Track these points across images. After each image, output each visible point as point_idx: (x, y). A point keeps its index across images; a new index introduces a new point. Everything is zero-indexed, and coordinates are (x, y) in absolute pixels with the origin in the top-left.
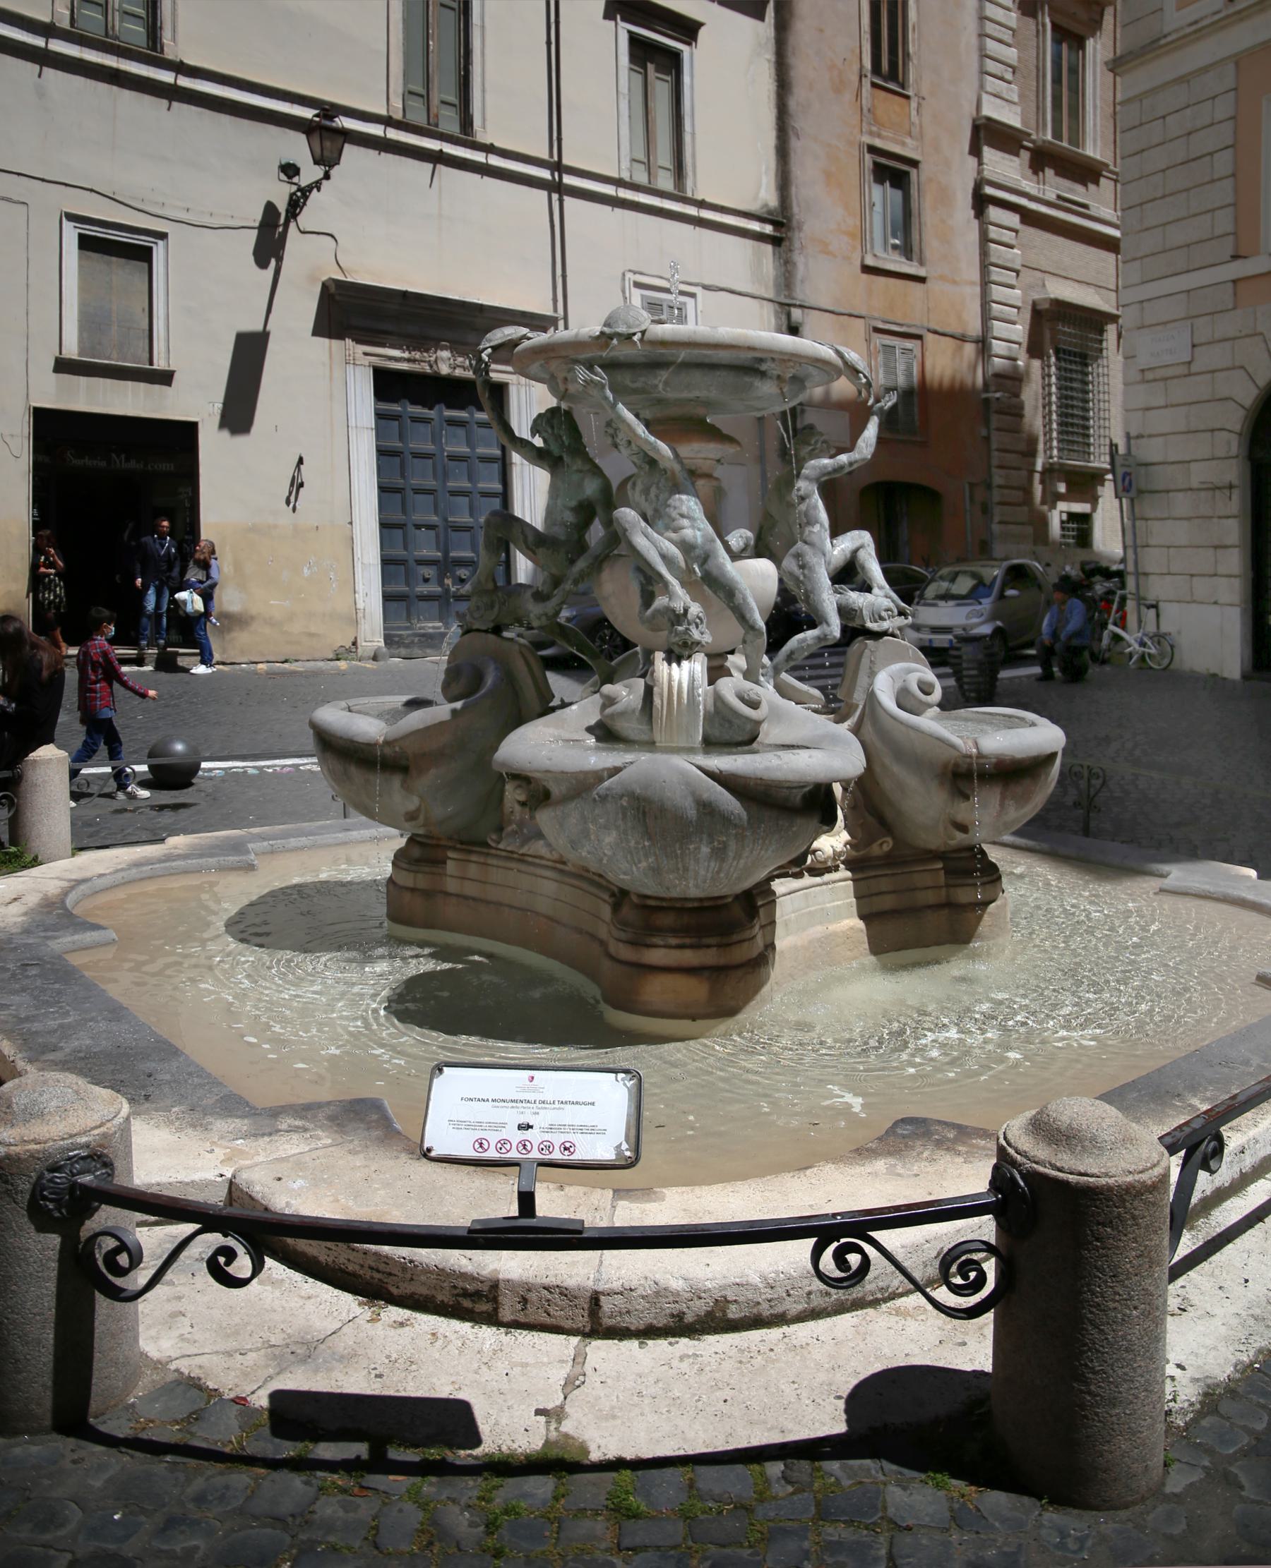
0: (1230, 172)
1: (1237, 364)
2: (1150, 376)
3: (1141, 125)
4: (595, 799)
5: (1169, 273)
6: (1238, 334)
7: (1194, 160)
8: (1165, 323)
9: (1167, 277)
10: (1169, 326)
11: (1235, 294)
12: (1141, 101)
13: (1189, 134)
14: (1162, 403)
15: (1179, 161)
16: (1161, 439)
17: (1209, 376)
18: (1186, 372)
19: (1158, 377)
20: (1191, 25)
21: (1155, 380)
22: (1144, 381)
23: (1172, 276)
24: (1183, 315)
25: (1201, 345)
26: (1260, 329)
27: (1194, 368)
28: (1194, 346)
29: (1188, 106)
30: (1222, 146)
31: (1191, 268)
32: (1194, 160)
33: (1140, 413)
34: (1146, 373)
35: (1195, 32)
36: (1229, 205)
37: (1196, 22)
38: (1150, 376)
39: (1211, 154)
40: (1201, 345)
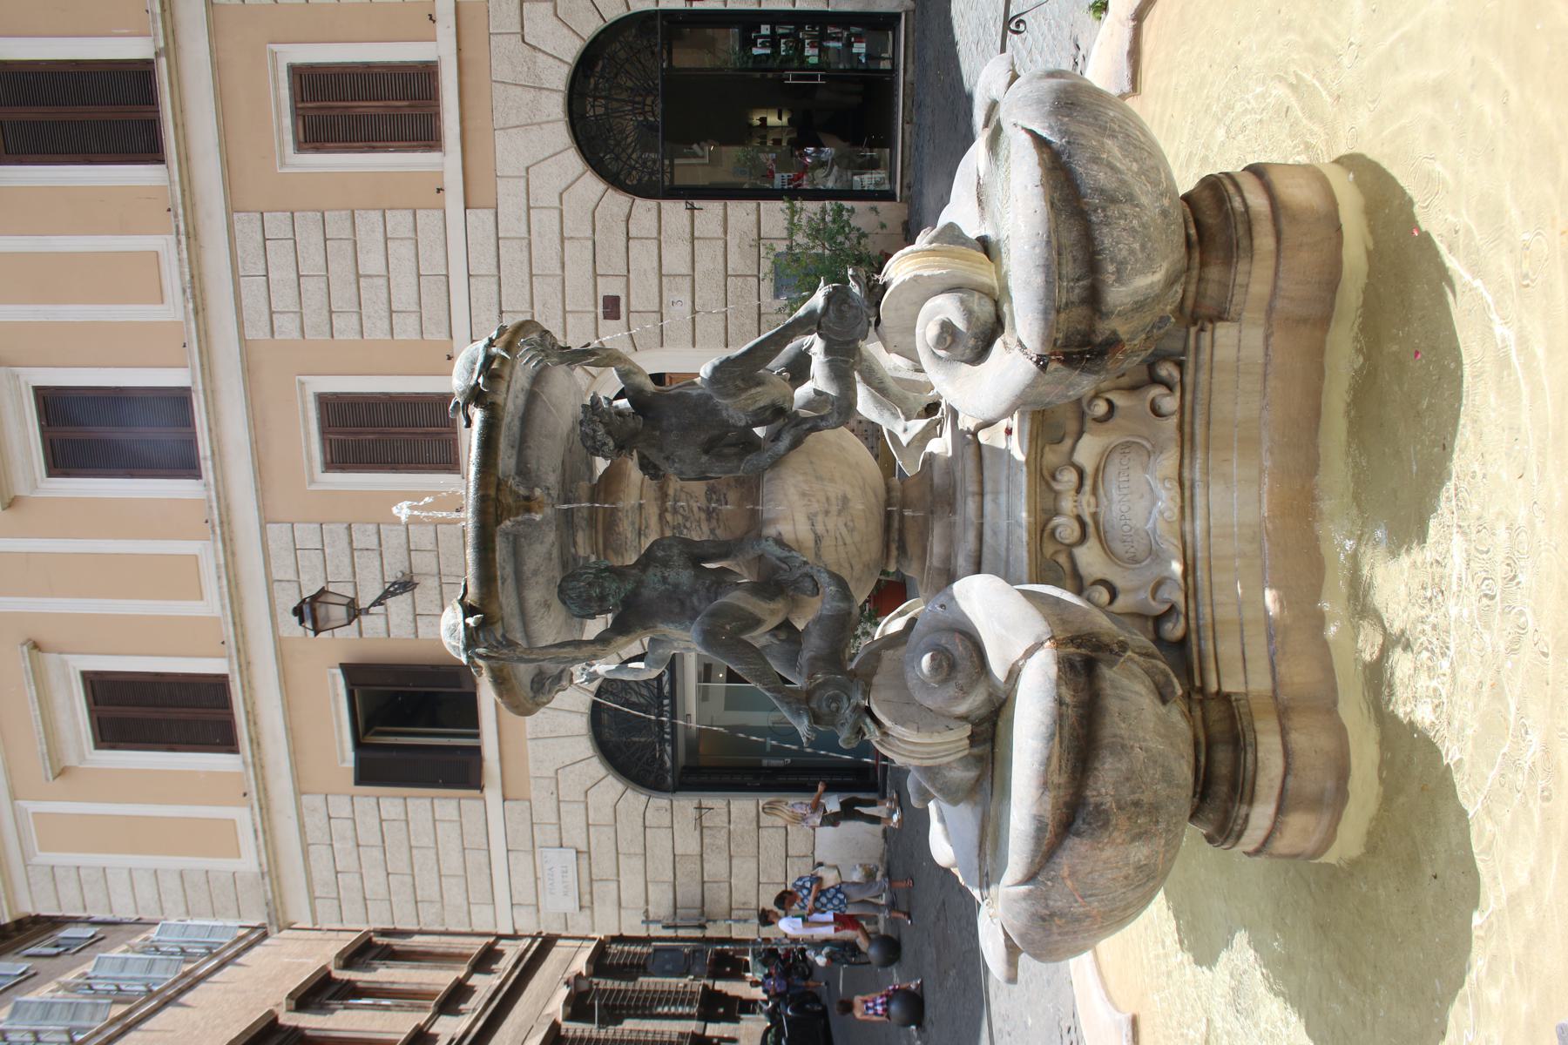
0: (402, 801)
1: (582, 798)
2: (586, 898)
3: (339, 900)
4: (1068, 142)
5: (488, 871)
6: (555, 796)
7: (383, 842)
8: (536, 879)
9: (491, 875)
10: (539, 875)
11: (517, 800)
12: (315, 898)
13: (358, 846)
14: (614, 885)
15: (382, 857)
16: (650, 887)
17: (592, 830)
18: (586, 856)
19: (588, 889)
20: (256, 837)
21: (591, 893)
22: (592, 908)
23: (491, 869)
24: (530, 857)
25: (561, 839)
26: (552, 774)
27: (583, 848)
28: (561, 846)
29: (332, 845)
30: (376, 809)
31: (486, 847)
32: (383, 842)
33: (622, 912)
34: (583, 903)
35: (264, 832)
36: (432, 804)
37: (256, 831)
38: (586, 898)
39: (381, 821)
40: (561, 839)
